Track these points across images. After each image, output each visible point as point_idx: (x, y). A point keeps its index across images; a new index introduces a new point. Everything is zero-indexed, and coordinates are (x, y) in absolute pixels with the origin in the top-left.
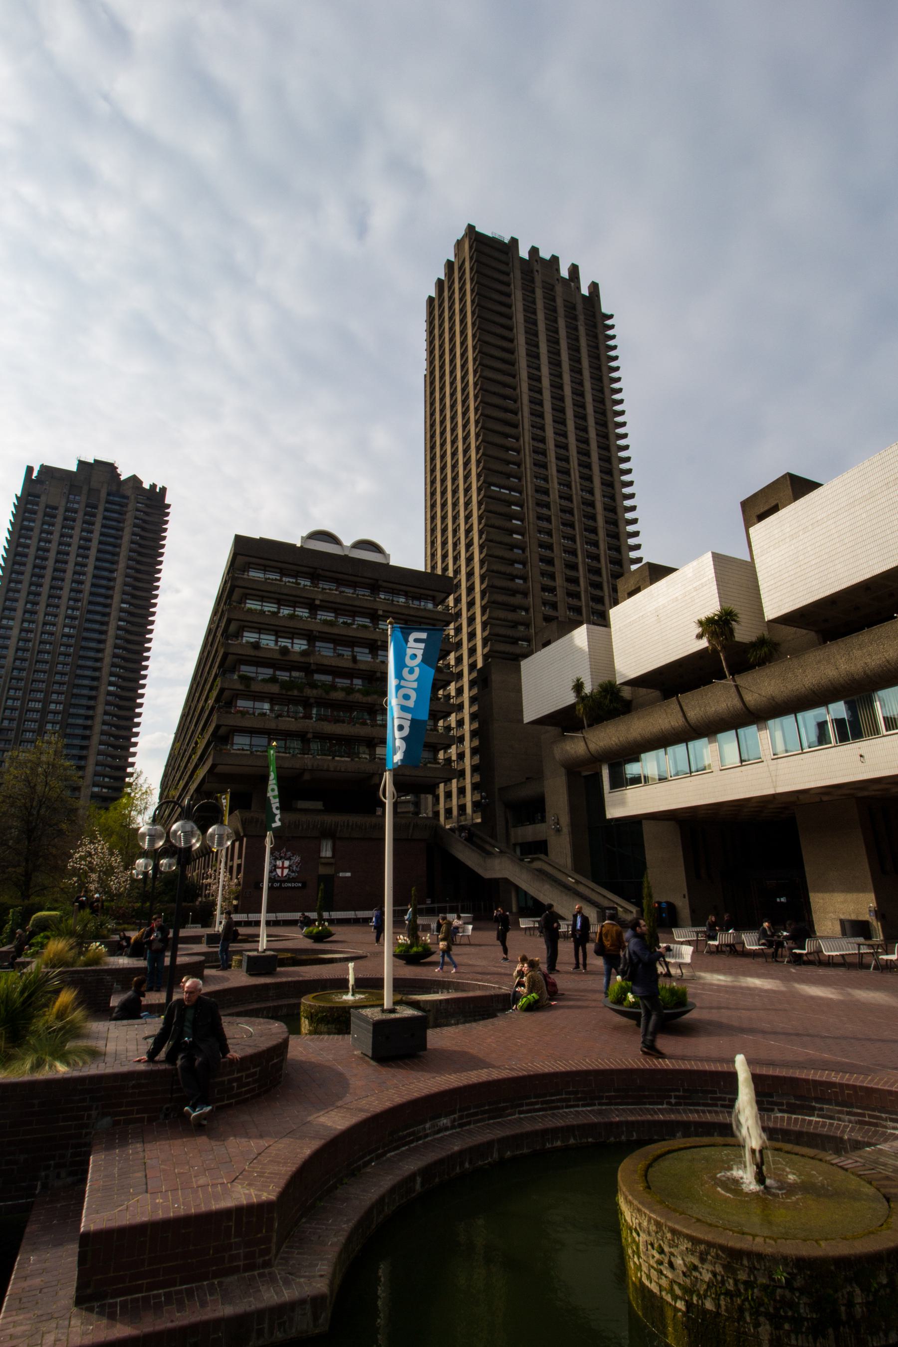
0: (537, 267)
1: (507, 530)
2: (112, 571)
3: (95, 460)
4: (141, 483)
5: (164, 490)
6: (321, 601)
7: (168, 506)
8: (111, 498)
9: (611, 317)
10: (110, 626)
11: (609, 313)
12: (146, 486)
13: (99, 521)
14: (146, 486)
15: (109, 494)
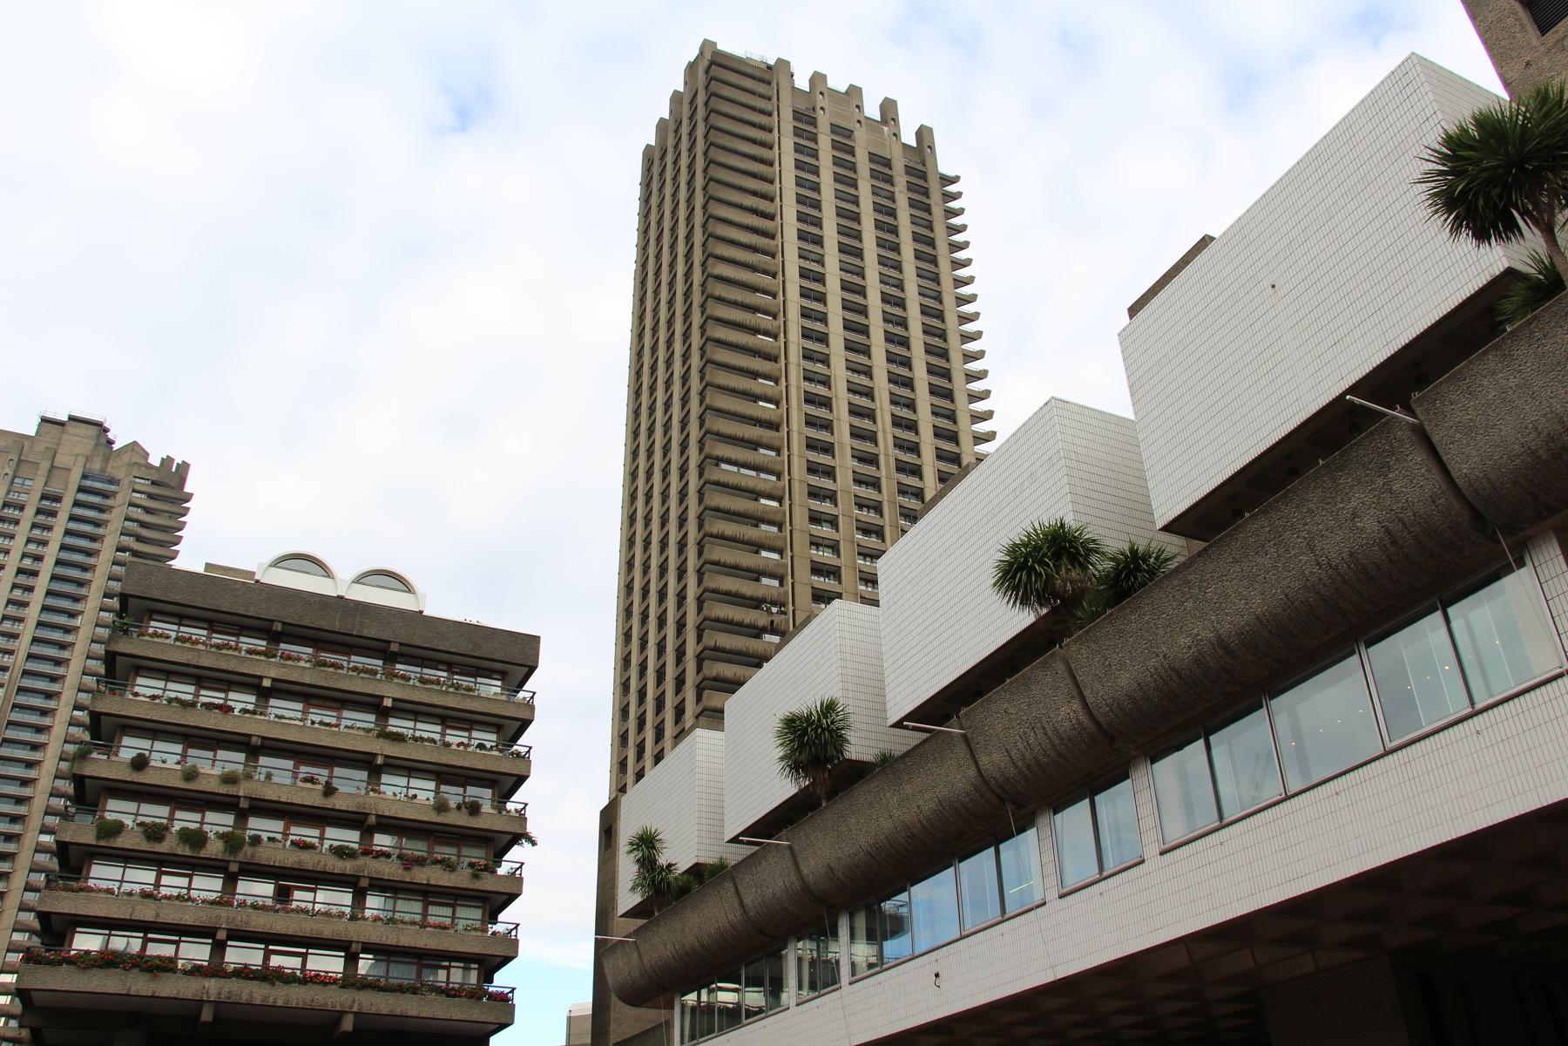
0: (821, 101)
1: (749, 543)
2: (72, 615)
3: (71, 418)
4: (147, 455)
5: (184, 467)
6: (274, 680)
7: (188, 497)
8: (88, 483)
9: (954, 180)
10: (57, 718)
11: (951, 173)
12: (155, 461)
13: (61, 523)
14: (155, 461)
15: (84, 477)
